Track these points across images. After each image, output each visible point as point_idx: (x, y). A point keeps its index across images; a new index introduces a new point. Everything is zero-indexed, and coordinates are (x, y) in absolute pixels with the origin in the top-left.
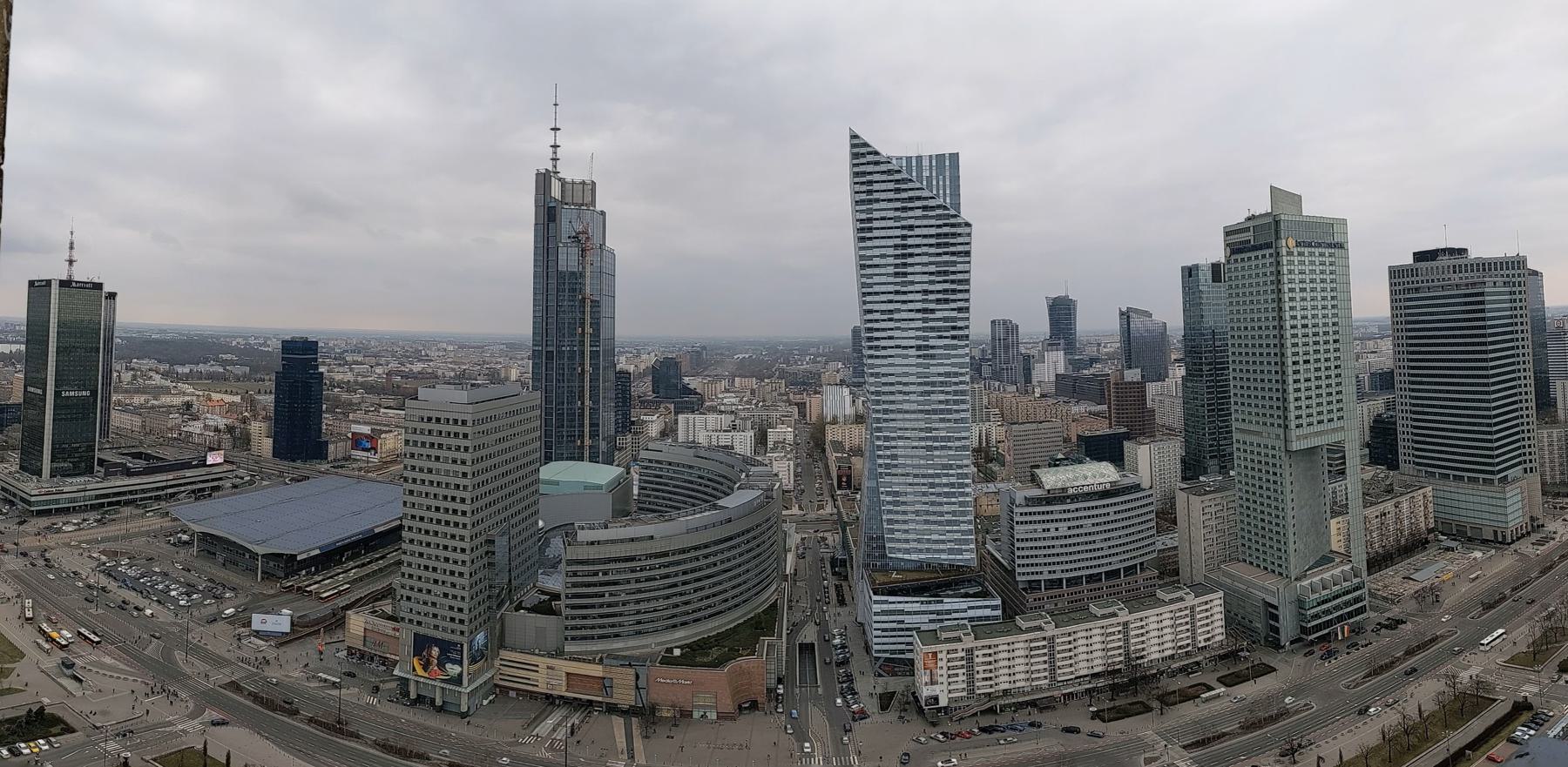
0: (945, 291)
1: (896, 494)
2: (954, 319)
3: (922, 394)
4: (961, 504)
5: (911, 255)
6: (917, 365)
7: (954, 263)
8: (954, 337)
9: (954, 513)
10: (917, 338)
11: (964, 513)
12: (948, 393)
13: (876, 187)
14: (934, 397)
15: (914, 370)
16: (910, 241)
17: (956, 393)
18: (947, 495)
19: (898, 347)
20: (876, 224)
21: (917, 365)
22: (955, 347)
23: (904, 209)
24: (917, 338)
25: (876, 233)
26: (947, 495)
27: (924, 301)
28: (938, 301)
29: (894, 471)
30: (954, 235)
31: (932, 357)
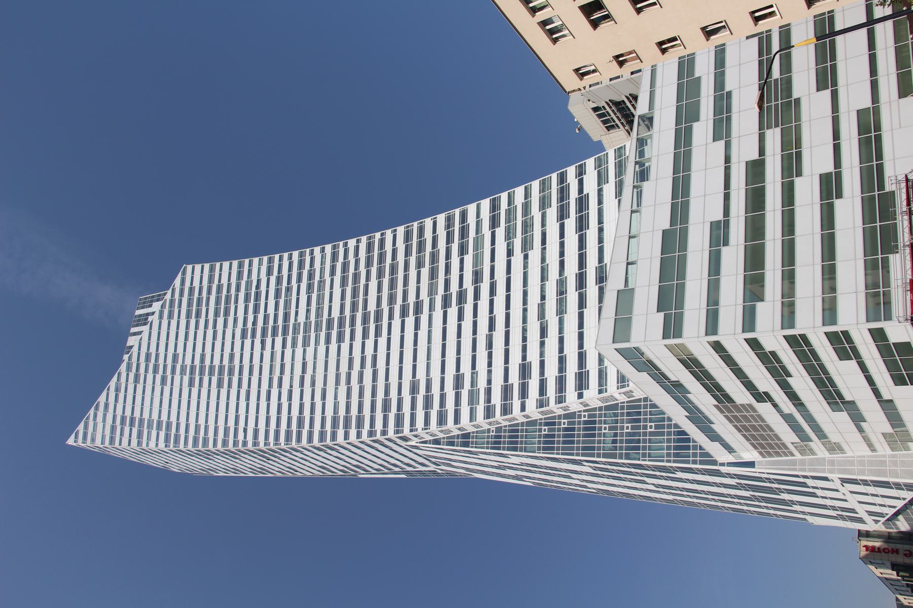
0: (247, 299)
1: (525, 370)
2: (279, 280)
3: (365, 335)
4: (544, 204)
5: (203, 357)
6: (328, 341)
7: (220, 287)
8: (299, 280)
9: (563, 215)
10: (294, 345)
11: (563, 193)
12: (368, 279)
13: (128, 413)
14: (372, 307)
15: (333, 347)
16: (188, 362)
17: (369, 263)
18: (527, 245)
19: (302, 384)
20: (164, 418)
21: (328, 341)
22: (311, 276)
23: (156, 371)
24: (294, 345)
25: (173, 418)
26: (527, 245)
27: (254, 336)
28: (256, 310)
29: (482, 384)
30: (191, 290)
31: (319, 314)
